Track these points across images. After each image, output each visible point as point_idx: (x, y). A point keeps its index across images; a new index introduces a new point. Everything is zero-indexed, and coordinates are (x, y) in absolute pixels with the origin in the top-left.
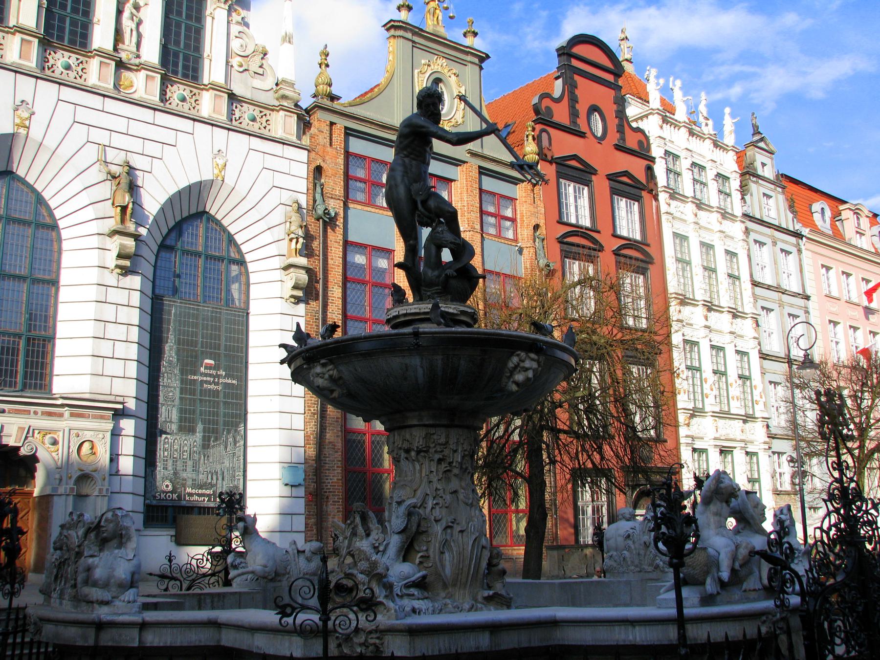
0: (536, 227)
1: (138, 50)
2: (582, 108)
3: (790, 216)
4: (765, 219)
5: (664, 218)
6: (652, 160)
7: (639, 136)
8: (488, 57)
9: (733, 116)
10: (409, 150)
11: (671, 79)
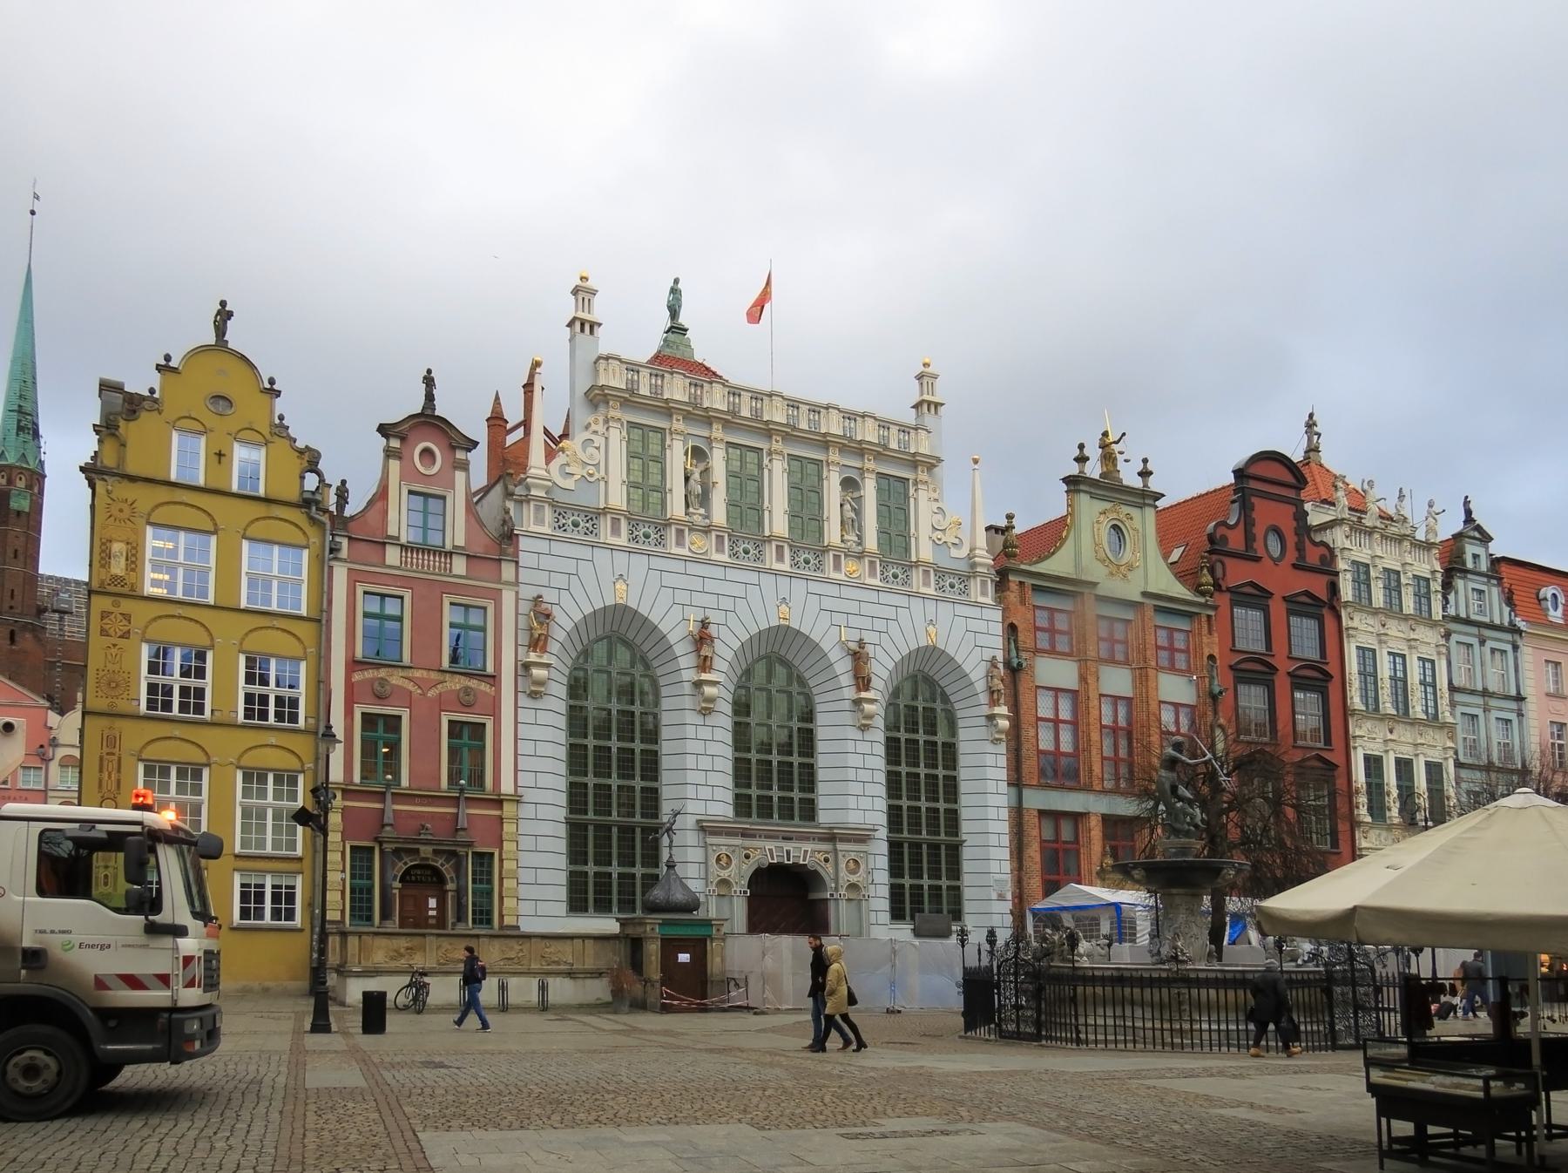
1: (859, 537)
2: (1259, 530)
3: (1507, 610)
4: (1473, 617)
6: (1337, 574)
7: (1323, 550)
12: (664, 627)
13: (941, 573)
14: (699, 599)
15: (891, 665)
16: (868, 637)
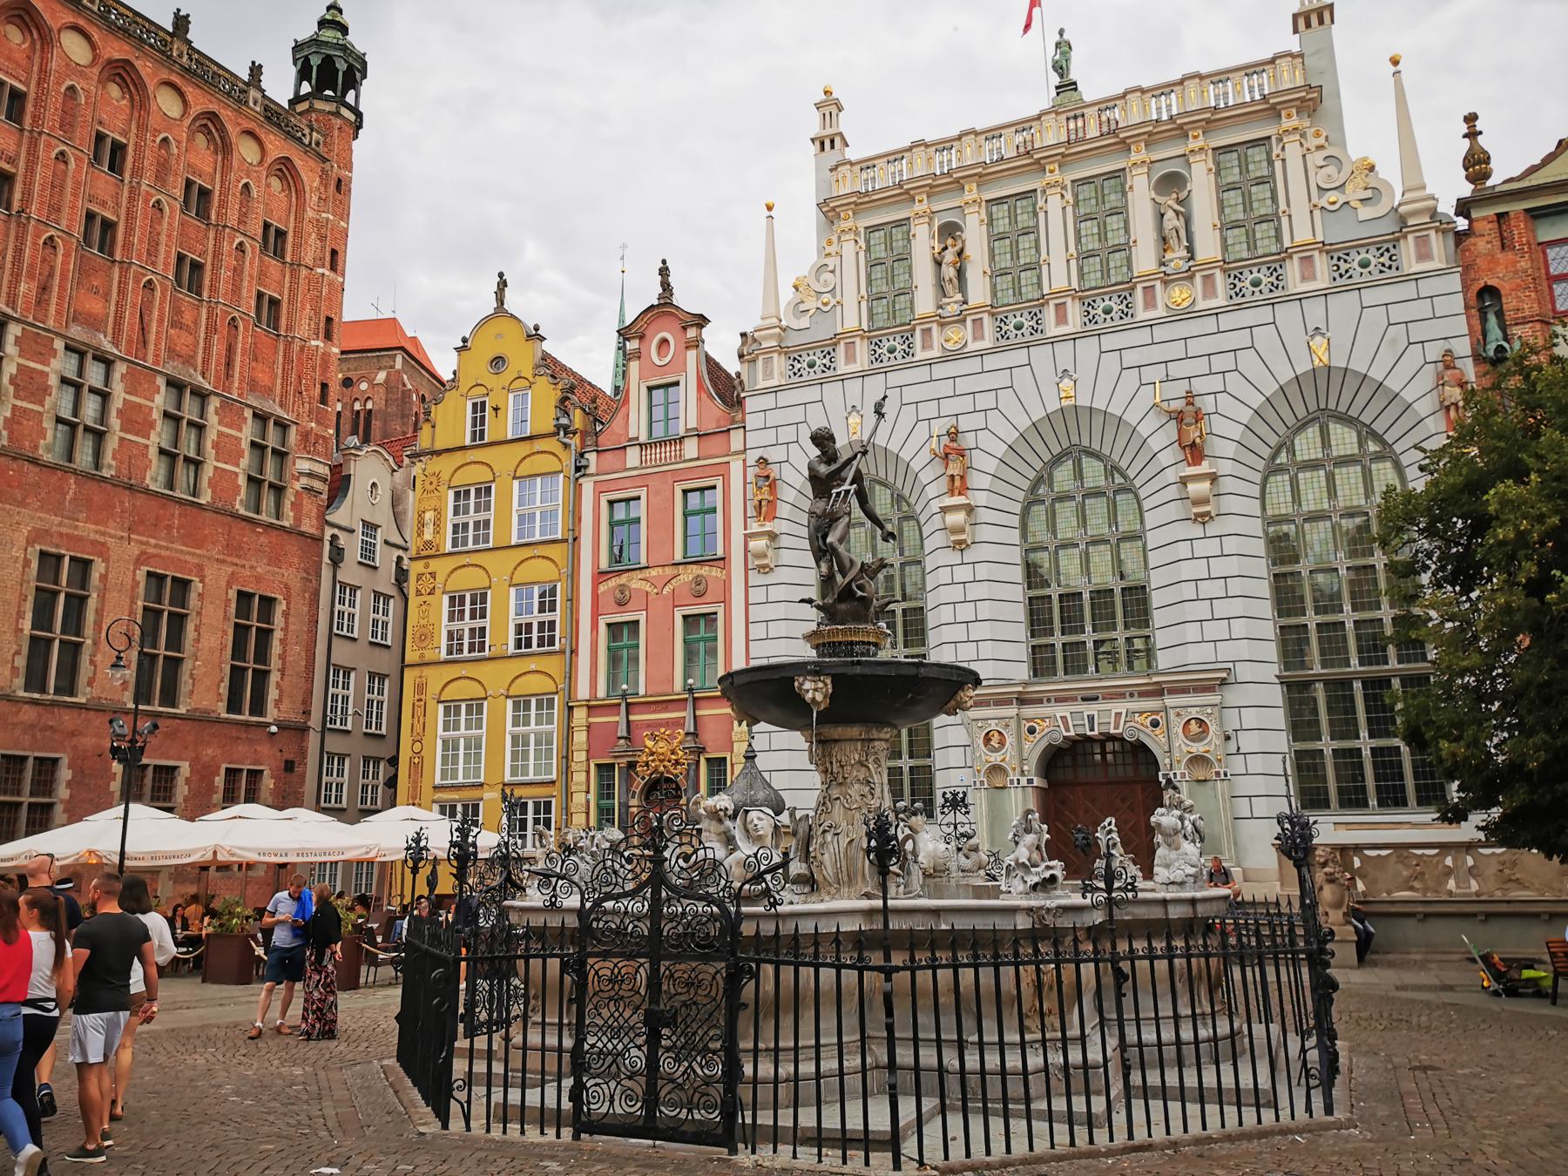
1: (1190, 249)
12: (905, 455)
13: (1337, 252)
14: (949, 407)
15: (1245, 415)
16: (1199, 386)
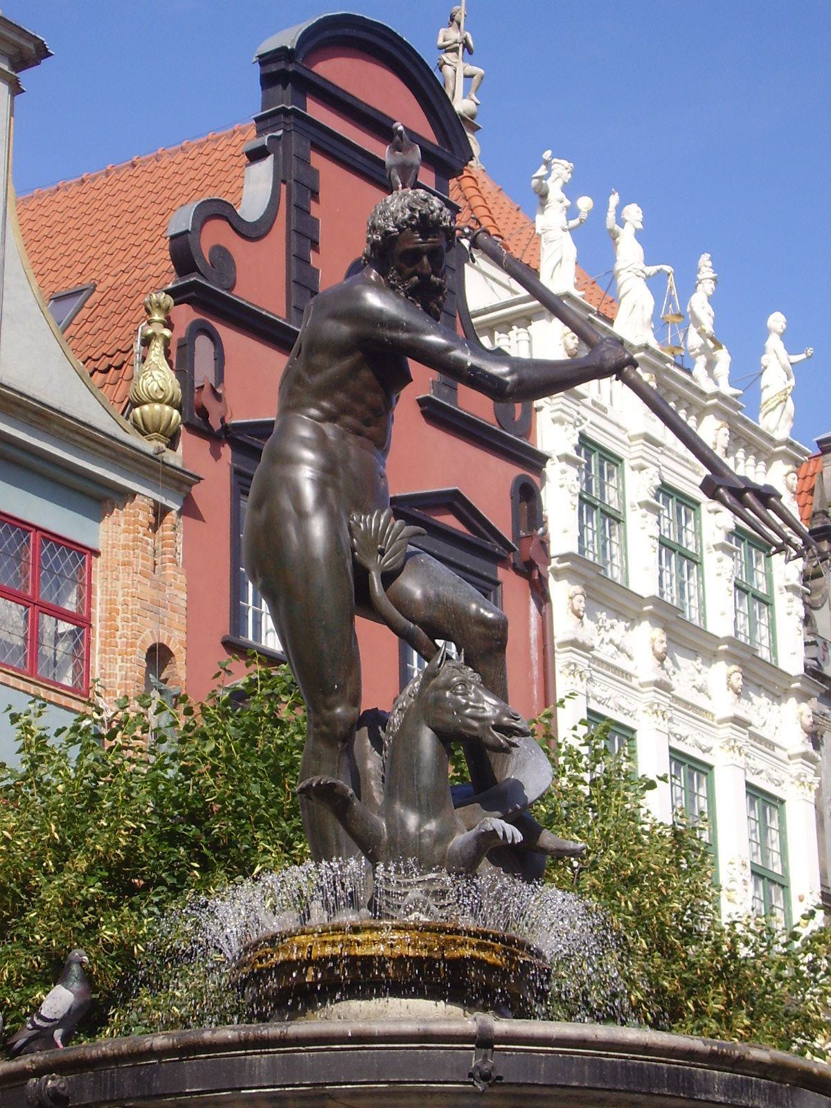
0: (158, 656)
5: (561, 659)
6: (535, 461)
8: (42, 52)
9: (791, 341)
10: (340, 396)
11: (614, 200)
